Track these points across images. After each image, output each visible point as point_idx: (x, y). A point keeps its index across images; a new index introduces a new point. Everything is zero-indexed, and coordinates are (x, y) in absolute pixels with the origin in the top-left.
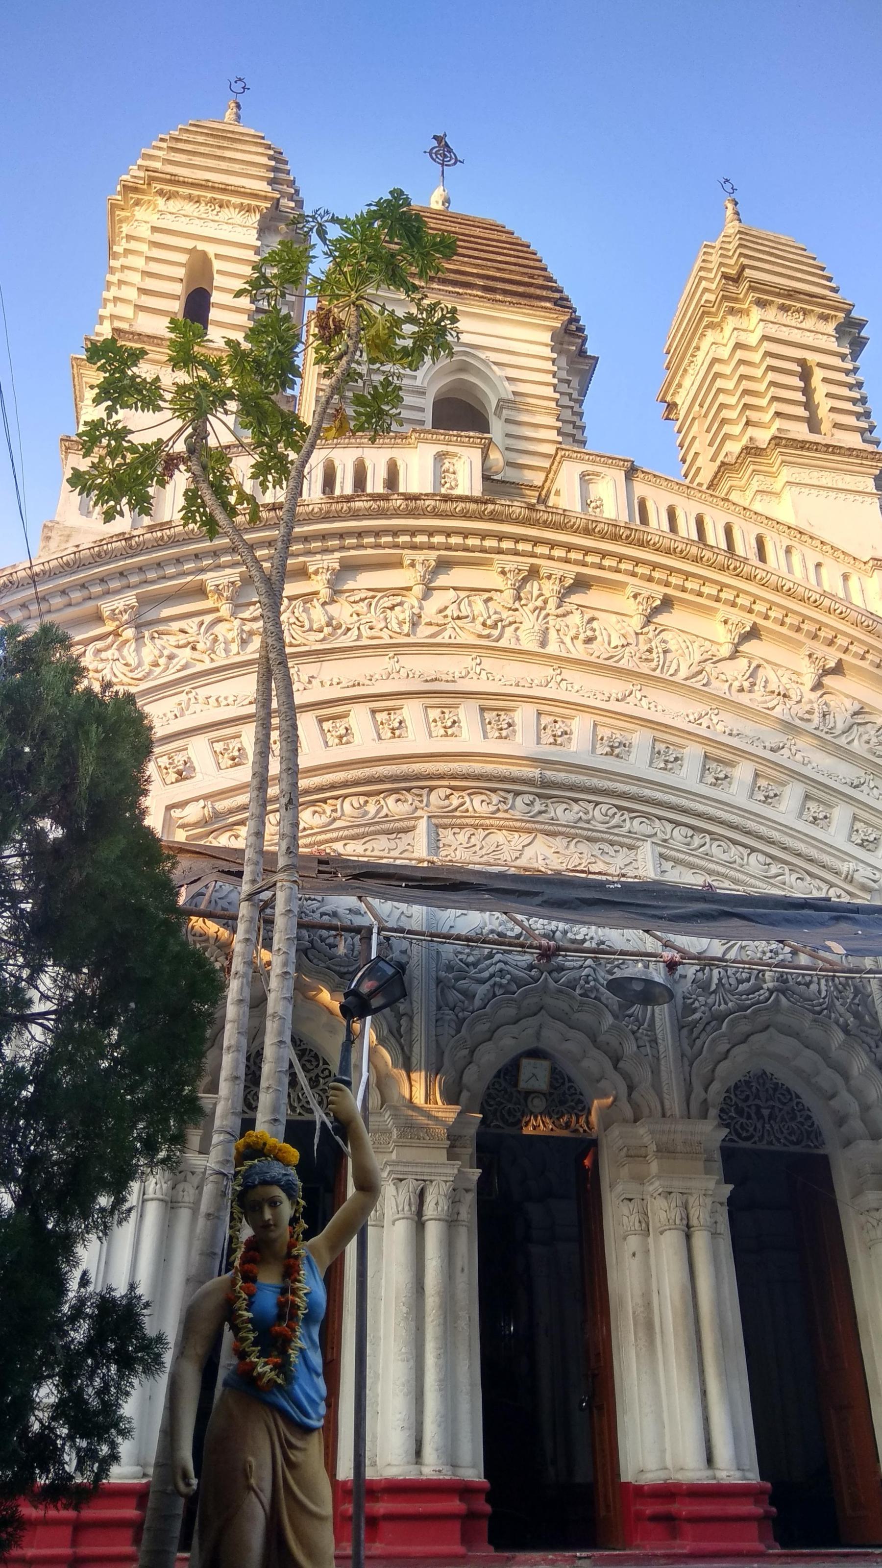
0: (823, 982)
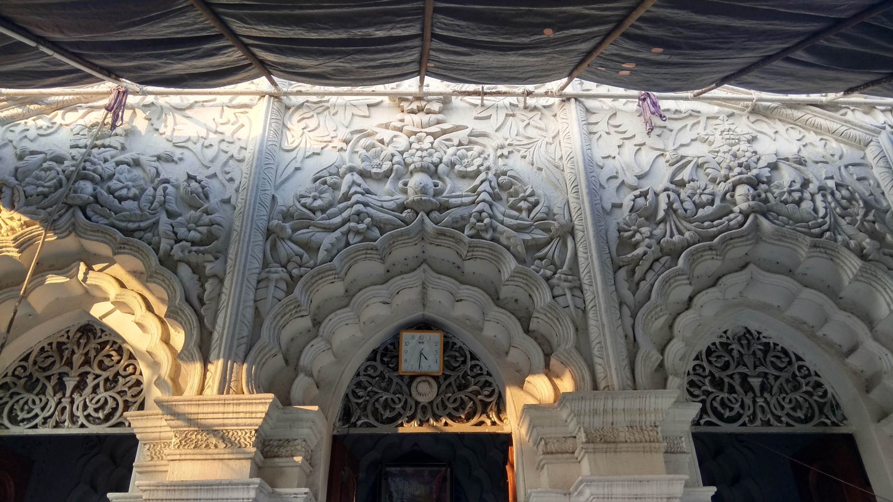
0: (819, 198)
